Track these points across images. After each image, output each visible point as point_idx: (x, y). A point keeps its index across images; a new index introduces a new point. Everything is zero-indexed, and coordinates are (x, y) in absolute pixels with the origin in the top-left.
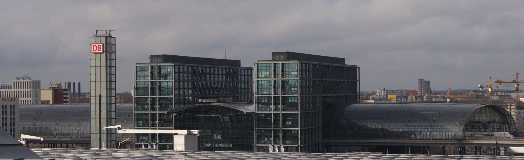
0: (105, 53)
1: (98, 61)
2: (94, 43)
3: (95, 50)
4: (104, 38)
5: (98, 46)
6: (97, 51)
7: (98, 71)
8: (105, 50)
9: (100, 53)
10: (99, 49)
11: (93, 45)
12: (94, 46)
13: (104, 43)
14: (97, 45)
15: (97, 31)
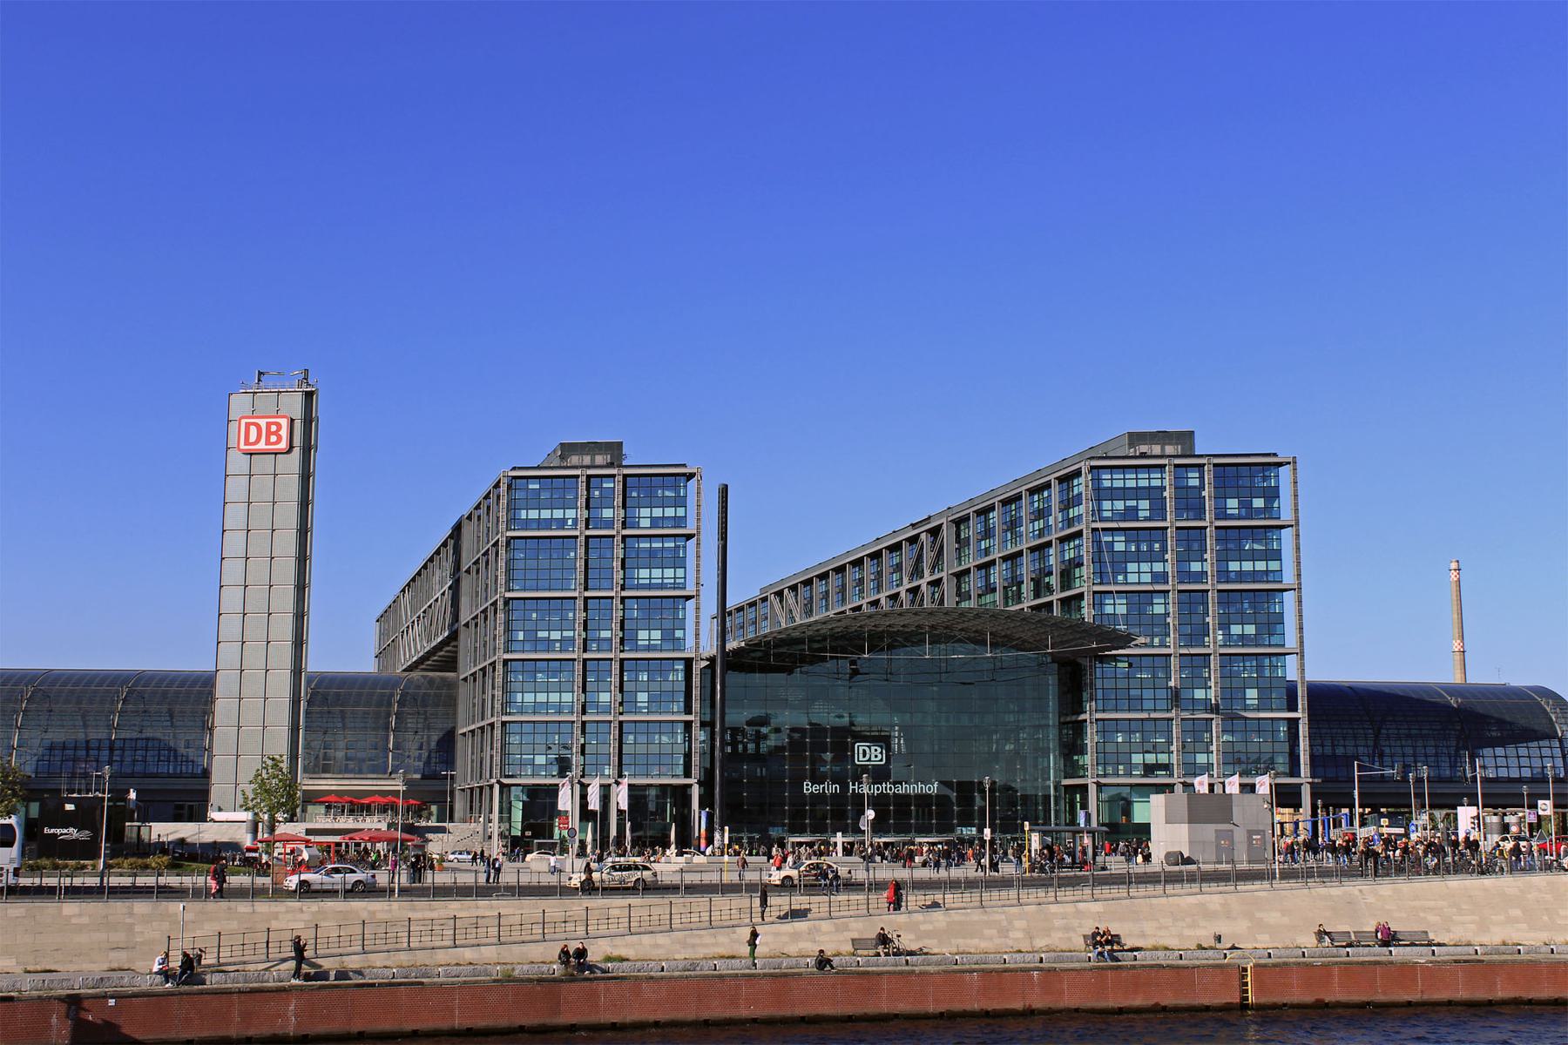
0: (297, 451)
1: (262, 486)
2: (244, 415)
3: (253, 438)
4: (298, 400)
5: (269, 425)
6: (262, 446)
7: (261, 519)
8: (297, 441)
9: (276, 454)
10: (273, 438)
11: (243, 422)
12: (248, 425)
13: (297, 412)
14: (263, 423)
15: (260, 373)
